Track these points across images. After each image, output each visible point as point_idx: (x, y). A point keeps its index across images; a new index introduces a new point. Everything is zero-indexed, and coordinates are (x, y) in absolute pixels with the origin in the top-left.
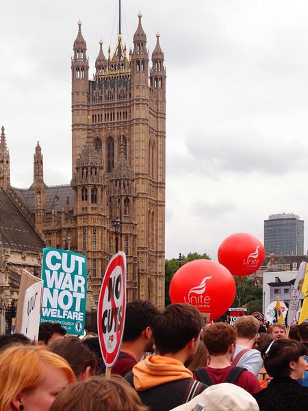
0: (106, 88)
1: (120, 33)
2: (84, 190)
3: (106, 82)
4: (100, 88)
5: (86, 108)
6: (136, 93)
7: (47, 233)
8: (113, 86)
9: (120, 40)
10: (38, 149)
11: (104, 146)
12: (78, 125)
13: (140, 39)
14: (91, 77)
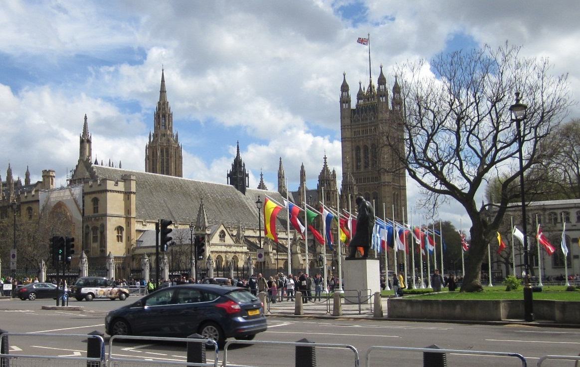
0: (362, 113)
1: (371, 77)
4: (358, 114)
5: (350, 127)
9: (371, 82)
10: (302, 167)
11: (362, 151)
12: (345, 138)
13: (382, 80)
14: (353, 105)
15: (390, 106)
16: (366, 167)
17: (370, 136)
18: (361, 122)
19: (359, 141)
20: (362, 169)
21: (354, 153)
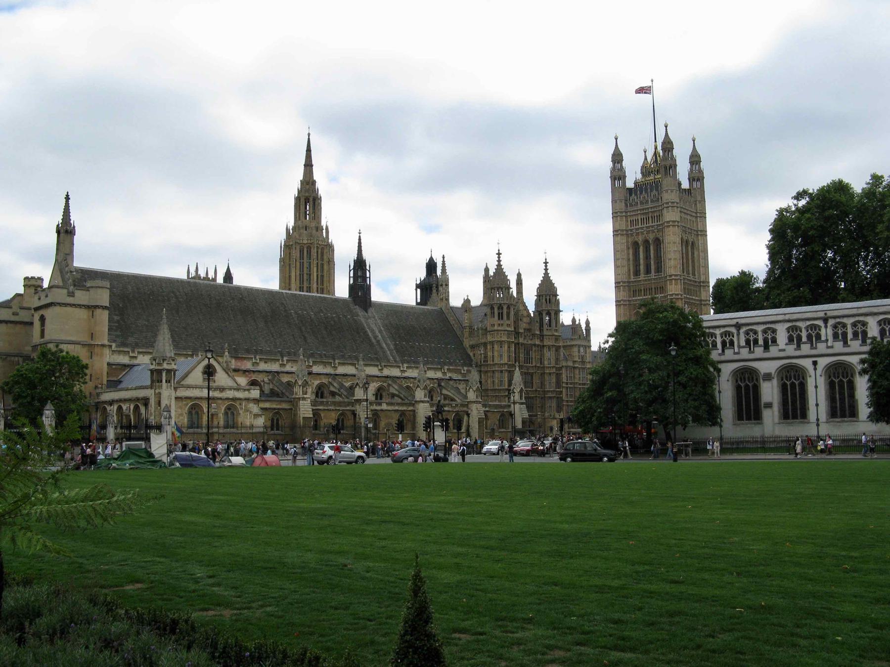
2: (492, 308)
3: (651, 186)
6: (667, 197)
7: (473, 347)
8: (646, 192)
13: (668, 146)
15: (685, 185)
16: (648, 271)
17: (652, 227)
18: (639, 207)
19: (638, 234)
20: (642, 277)
21: (631, 252)
